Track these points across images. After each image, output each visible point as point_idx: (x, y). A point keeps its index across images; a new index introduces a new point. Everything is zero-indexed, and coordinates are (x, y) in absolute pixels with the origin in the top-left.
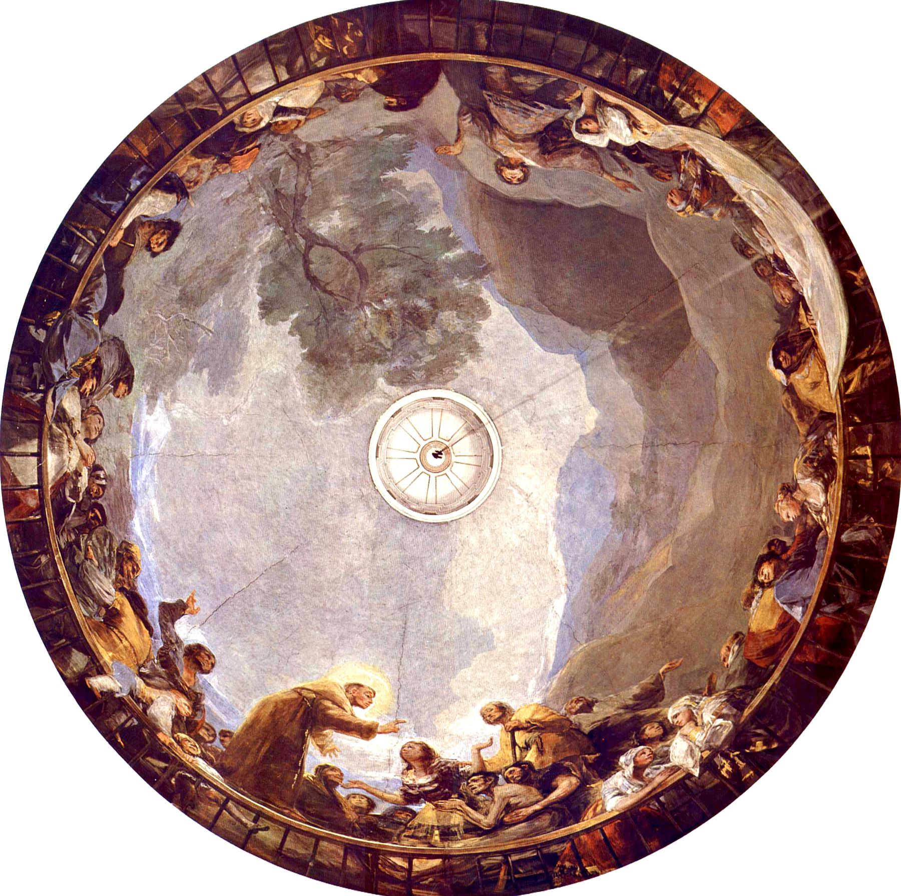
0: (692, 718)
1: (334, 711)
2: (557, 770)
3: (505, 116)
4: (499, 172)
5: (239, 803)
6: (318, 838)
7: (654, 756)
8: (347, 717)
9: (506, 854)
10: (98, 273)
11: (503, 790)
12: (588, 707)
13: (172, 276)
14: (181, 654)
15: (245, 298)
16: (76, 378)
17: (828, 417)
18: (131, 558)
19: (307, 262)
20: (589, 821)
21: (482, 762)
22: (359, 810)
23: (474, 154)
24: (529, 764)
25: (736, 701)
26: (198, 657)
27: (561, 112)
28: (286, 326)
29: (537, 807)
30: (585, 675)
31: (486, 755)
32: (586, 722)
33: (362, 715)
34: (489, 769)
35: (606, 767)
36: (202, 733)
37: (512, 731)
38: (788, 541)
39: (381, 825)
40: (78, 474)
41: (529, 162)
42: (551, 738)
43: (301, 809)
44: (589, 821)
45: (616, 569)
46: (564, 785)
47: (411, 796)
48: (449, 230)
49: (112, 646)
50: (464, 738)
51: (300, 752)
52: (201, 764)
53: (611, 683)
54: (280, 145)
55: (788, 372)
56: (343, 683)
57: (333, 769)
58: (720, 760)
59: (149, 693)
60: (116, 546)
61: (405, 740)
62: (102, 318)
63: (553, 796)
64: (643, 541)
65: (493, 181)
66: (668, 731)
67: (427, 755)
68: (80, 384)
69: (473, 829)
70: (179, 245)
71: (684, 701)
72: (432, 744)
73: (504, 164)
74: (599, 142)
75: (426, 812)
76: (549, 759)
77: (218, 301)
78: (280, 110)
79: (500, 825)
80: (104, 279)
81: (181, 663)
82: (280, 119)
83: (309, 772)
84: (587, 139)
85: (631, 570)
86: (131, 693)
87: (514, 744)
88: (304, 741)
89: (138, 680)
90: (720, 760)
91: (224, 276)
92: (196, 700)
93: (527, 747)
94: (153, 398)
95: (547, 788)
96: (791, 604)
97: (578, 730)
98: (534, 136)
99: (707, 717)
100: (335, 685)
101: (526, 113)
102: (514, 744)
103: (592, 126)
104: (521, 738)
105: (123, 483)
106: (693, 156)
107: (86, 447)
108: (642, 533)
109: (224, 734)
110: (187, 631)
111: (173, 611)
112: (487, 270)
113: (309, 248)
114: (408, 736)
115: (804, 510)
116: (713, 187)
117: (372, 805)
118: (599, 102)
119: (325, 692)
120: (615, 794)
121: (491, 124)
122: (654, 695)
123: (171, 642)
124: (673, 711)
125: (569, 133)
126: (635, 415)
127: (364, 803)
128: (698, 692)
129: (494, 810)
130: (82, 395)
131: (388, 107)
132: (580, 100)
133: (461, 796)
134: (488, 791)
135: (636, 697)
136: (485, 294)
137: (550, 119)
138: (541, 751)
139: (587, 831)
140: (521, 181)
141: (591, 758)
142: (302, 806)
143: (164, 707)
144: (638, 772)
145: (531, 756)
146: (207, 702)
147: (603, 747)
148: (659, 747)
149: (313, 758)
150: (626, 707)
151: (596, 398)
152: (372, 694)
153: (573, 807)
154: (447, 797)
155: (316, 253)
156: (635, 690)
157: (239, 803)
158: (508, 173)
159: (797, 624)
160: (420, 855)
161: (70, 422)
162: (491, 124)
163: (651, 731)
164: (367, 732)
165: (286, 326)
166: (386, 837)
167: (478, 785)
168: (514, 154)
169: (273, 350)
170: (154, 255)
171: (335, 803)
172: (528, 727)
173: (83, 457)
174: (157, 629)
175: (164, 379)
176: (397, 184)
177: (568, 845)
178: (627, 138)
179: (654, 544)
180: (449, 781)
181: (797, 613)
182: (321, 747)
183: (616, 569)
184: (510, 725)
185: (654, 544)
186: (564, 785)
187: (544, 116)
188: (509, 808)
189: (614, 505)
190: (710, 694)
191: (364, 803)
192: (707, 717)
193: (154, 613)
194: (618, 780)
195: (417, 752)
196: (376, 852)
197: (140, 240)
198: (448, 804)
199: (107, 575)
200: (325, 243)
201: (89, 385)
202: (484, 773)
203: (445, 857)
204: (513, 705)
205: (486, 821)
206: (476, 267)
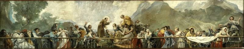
29: (129, 32)
33: (108, 22)
51: (104, 29)
67: (115, 25)
104: (126, 20)
129: (124, 32)
145: (127, 23)
149: (105, 29)
164: (108, 24)
184: (125, 18)
188: (125, 32)
205: (123, 34)
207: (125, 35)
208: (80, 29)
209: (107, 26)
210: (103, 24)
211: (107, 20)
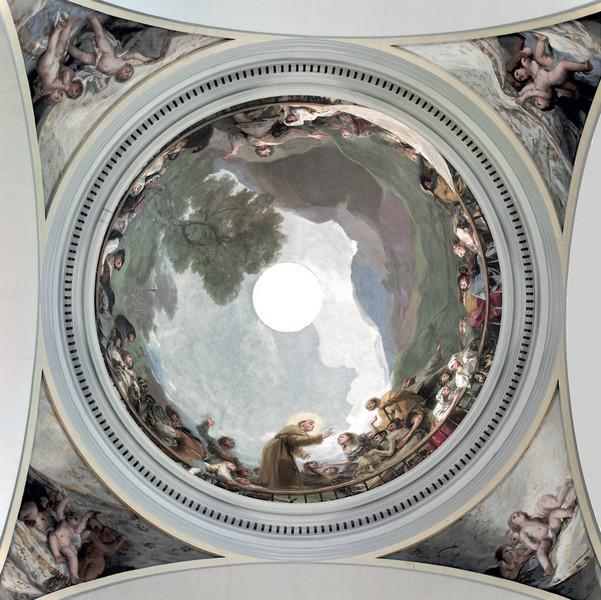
0: (459, 364)
1: (300, 438)
2: (411, 415)
3: (250, 131)
4: (259, 154)
5: (278, 494)
6: (320, 493)
7: (449, 389)
8: (306, 437)
9: (404, 461)
10: (101, 291)
11: (391, 436)
12: (413, 381)
13: (130, 274)
14: (217, 445)
15: (165, 267)
16: (113, 343)
17: (458, 203)
18: (174, 413)
19: (186, 236)
20: (434, 430)
21: (376, 428)
22: (331, 474)
23: (239, 147)
24: (398, 419)
25: (474, 348)
26: (225, 442)
27: (276, 119)
28: (189, 269)
29: (409, 435)
30: (403, 371)
31: (377, 424)
32: (415, 388)
33: (312, 434)
34: (381, 430)
35: (431, 403)
36: (246, 473)
37: (384, 408)
38: (466, 265)
39: (345, 475)
40: (133, 385)
41: (270, 144)
42: (402, 404)
43: (307, 485)
44: (434, 430)
45: (398, 312)
46: (416, 421)
47: (353, 457)
48: (245, 190)
49: (187, 454)
50: (362, 422)
51: (293, 463)
52: (253, 487)
53: (420, 365)
54: (151, 193)
55: (432, 190)
56: (296, 424)
57: (311, 463)
58: (477, 376)
59: (215, 467)
60: (164, 410)
61: (337, 436)
62: (110, 309)
63: (414, 427)
64: (404, 293)
65: (257, 159)
66: (451, 375)
67: (351, 437)
68: (115, 344)
69: (386, 458)
70: (127, 258)
71: (453, 358)
72: (350, 431)
73: (258, 149)
74: (300, 123)
75: (362, 461)
76: (405, 413)
77: (154, 273)
78: (147, 178)
79: (396, 450)
80: (104, 293)
81: (220, 448)
82: (149, 181)
83: (301, 468)
84: (292, 124)
85: (405, 309)
86: (207, 470)
87: (387, 414)
88: (292, 458)
89: (208, 465)
90: (477, 376)
91: (152, 261)
92: (235, 461)
93: (394, 412)
94: (146, 335)
95: (410, 426)
96: (479, 293)
97: (413, 394)
98: (268, 133)
99: (465, 360)
100: (292, 426)
101: (261, 126)
102: (387, 414)
103: (293, 118)
104: (389, 409)
105: (152, 379)
106: (346, 114)
107: (131, 372)
108: (402, 290)
109: (256, 470)
110: (214, 433)
111: (204, 427)
112: (273, 198)
113: (184, 229)
114: (339, 432)
115: (466, 248)
116: (360, 124)
117: (336, 469)
118: (291, 108)
119: (286, 431)
120: (440, 413)
121: (246, 135)
122: (441, 361)
123: (210, 442)
124: (452, 363)
125: (284, 125)
126: (372, 233)
127: (333, 470)
128: (457, 351)
129: (391, 445)
130: (118, 348)
131: (194, 152)
132: (283, 111)
133: (374, 448)
134: (385, 439)
135: (432, 367)
136: (277, 210)
137: (273, 123)
138: (400, 411)
139: (434, 434)
140: (271, 153)
141: (423, 403)
142: (306, 484)
143: (224, 470)
144: (445, 398)
146: (240, 460)
147: (427, 396)
148: (450, 384)
149: (300, 462)
150: (429, 373)
151: (351, 236)
152: (312, 423)
153: (425, 426)
154: (368, 450)
155: (188, 230)
156: (430, 364)
157: (278, 494)
158: (263, 153)
159: (485, 302)
160: (368, 479)
161: (119, 363)
162: (246, 135)
163: (444, 378)
164: (318, 440)
165: (189, 269)
166: (350, 478)
167: (379, 439)
168: (262, 143)
169: (188, 283)
170: (119, 269)
171: (319, 476)
172: (390, 403)
173: (132, 377)
174: (201, 438)
175: (147, 324)
176: (212, 180)
177: (428, 444)
178: (312, 117)
179: (410, 293)
180: (366, 443)
181: (483, 297)
182: (301, 456)
183: (398, 312)
184: (382, 405)
185: (410, 293)
186: (416, 421)
187: (269, 123)
188: (397, 442)
189: (384, 283)
190: (463, 348)
191: (333, 470)
192: (465, 360)
193: (196, 433)
194: (439, 407)
195: (345, 438)
196: (348, 486)
197: (111, 267)
198: (370, 453)
199: (168, 424)
200: (190, 223)
201: (118, 344)
202: (382, 433)
203: (379, 475)
204: (379, 395)
205: (390, 452)
206: (267, 199)
207: (396, 450)
208: (185, 430)
209: (306, 449)
210: (288, 444)
211: (306, 430)
